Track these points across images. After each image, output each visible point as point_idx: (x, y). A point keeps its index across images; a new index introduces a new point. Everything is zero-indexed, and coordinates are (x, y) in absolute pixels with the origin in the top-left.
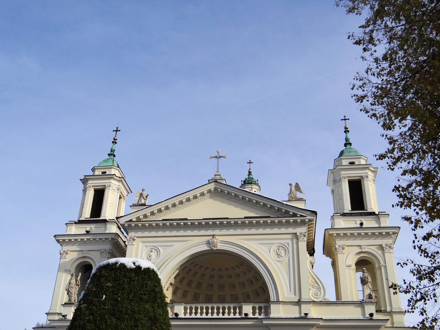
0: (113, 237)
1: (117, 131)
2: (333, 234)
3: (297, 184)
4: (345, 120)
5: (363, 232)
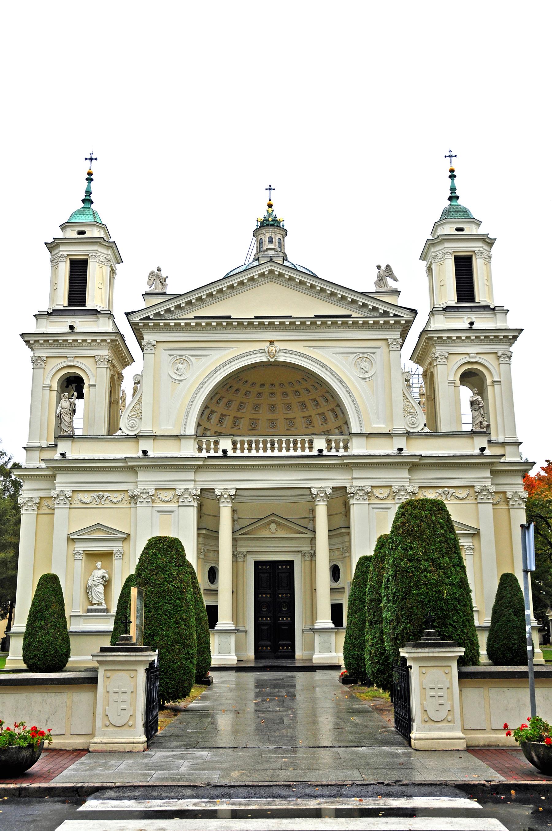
0: (114, 338)
1: (91, 159)
2: (432, 337)
3: (388, 266)
4: (450, 156)
5: (473, 335)
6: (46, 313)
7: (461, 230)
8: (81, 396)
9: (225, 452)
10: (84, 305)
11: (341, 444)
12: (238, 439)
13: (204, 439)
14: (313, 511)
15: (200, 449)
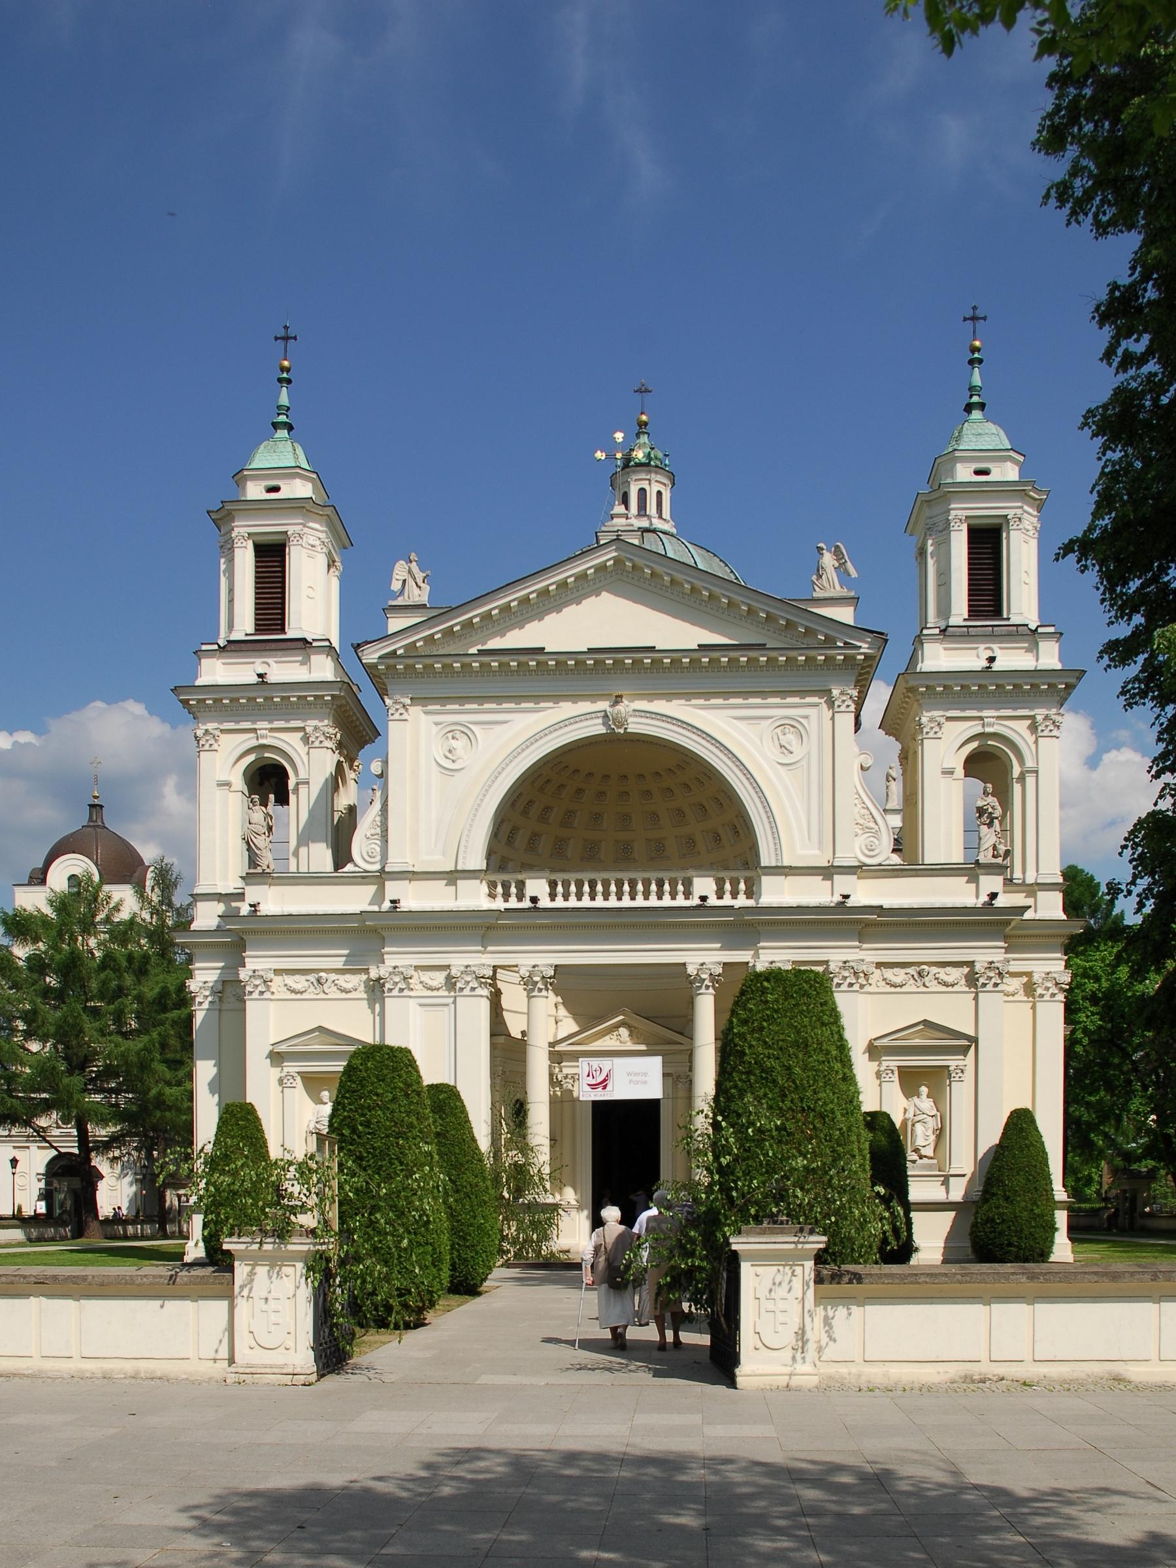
1: (286, 338)
4: (974, 318)
6: (216, 647)
7: (985, 472)
8: (283, 800)
9: (534, 900)
10: (283, 630)
11: (742, 886)
12: (559, 877)
13: (499, 878)
14: (691, 1004)
15: (492, 896)
